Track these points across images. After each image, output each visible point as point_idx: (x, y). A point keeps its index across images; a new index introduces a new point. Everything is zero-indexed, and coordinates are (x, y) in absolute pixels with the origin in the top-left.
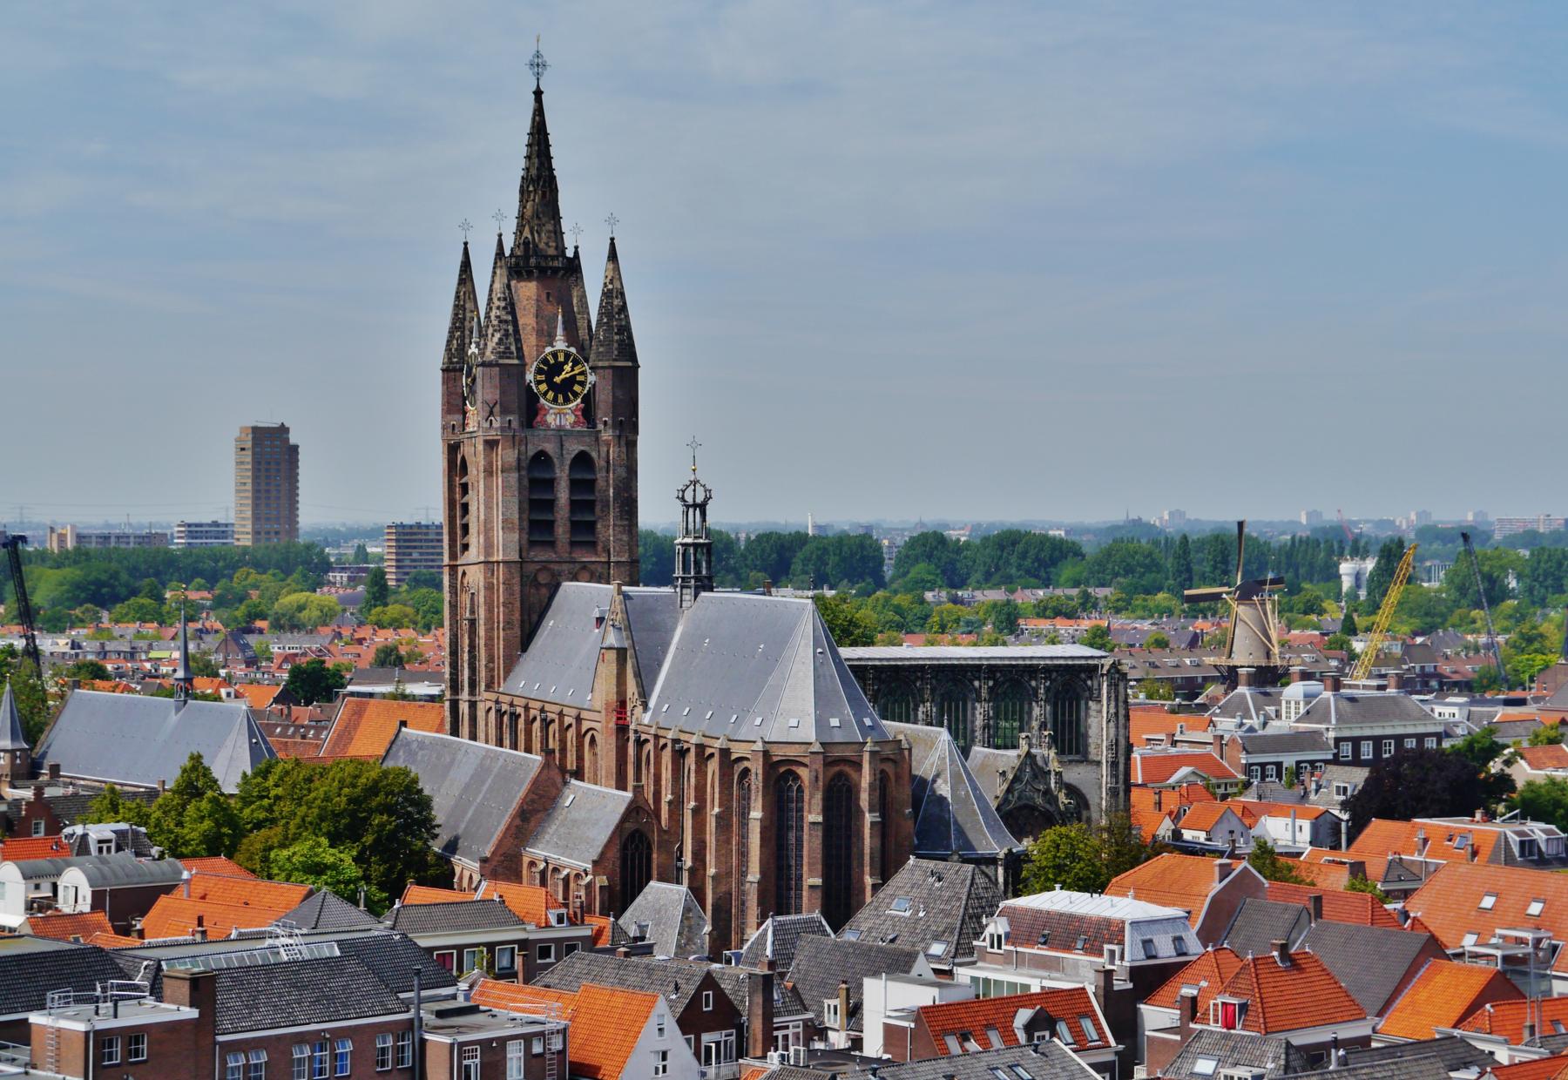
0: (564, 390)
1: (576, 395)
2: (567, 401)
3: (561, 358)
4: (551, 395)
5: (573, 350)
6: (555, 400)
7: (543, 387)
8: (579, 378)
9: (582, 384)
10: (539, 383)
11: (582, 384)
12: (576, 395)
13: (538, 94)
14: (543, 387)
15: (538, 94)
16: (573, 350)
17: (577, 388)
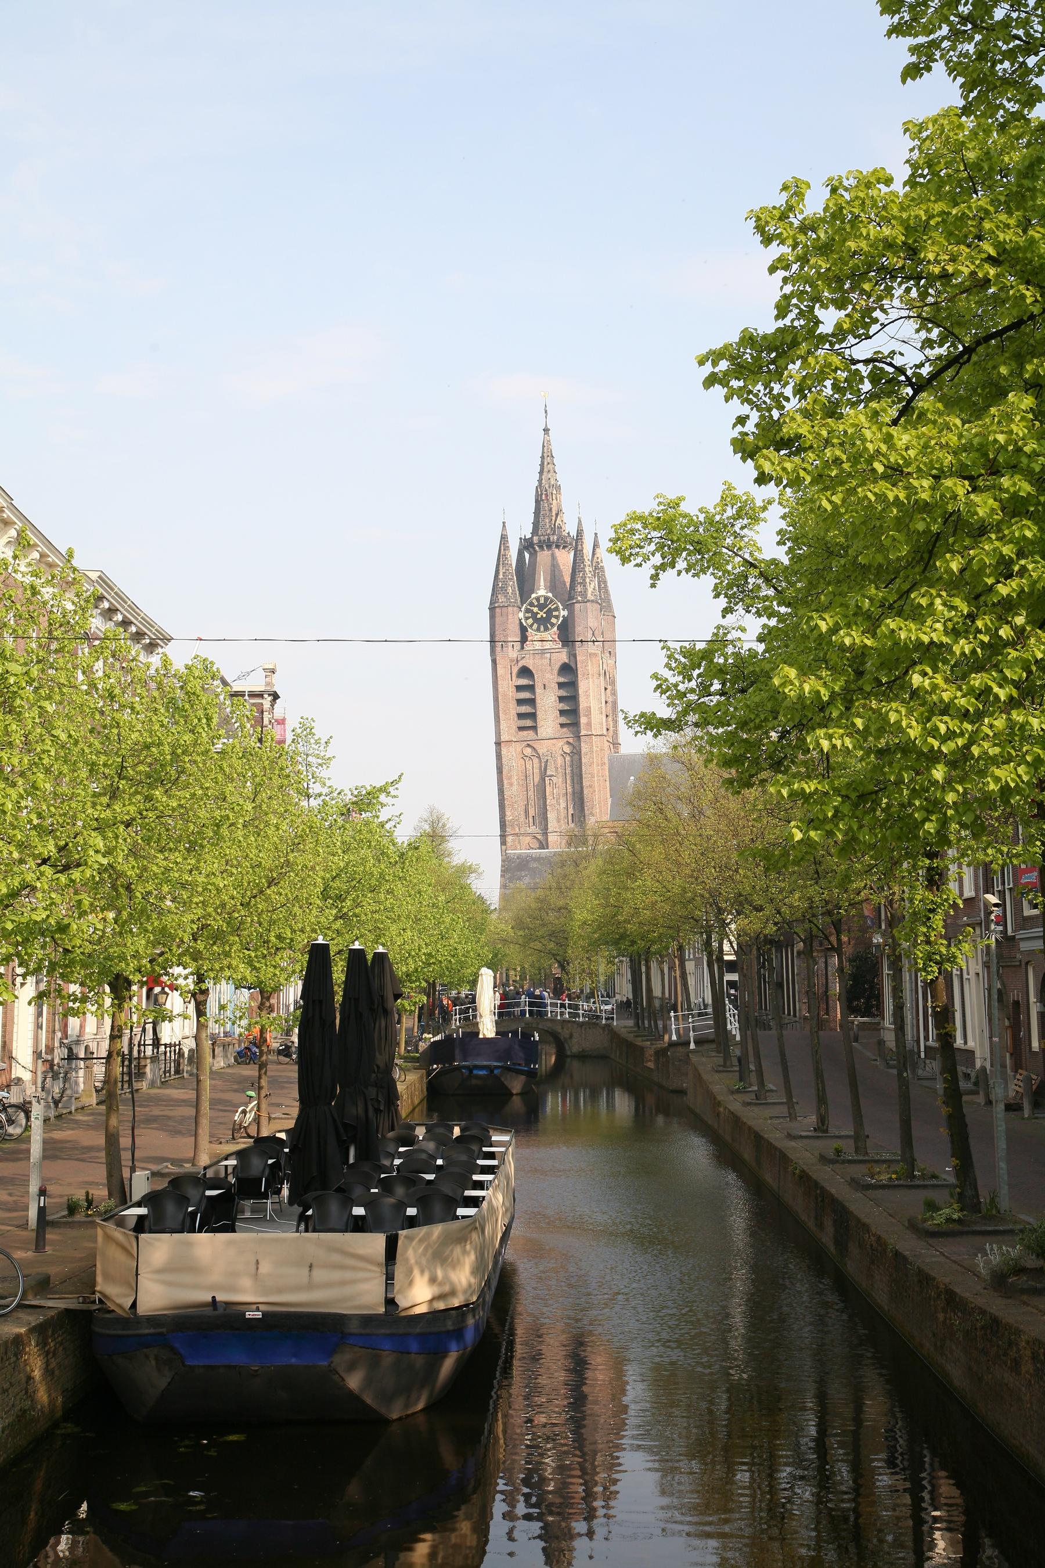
0: (544, 623)
1: (553, 625)
2: (546, 629)
3: (542, 601)
4: (535, 626)
5: (550, 595)
6: (538, 630)
7: (530, 621)
8: (554, 613)
9: (557, 617)
10: (527, 618)
11: (557, 617)
12: (553, 625)
13: (546, 430)
14: (530, 621)
15: (546, 430)
16: (550, 595)
17: (554, 620)
